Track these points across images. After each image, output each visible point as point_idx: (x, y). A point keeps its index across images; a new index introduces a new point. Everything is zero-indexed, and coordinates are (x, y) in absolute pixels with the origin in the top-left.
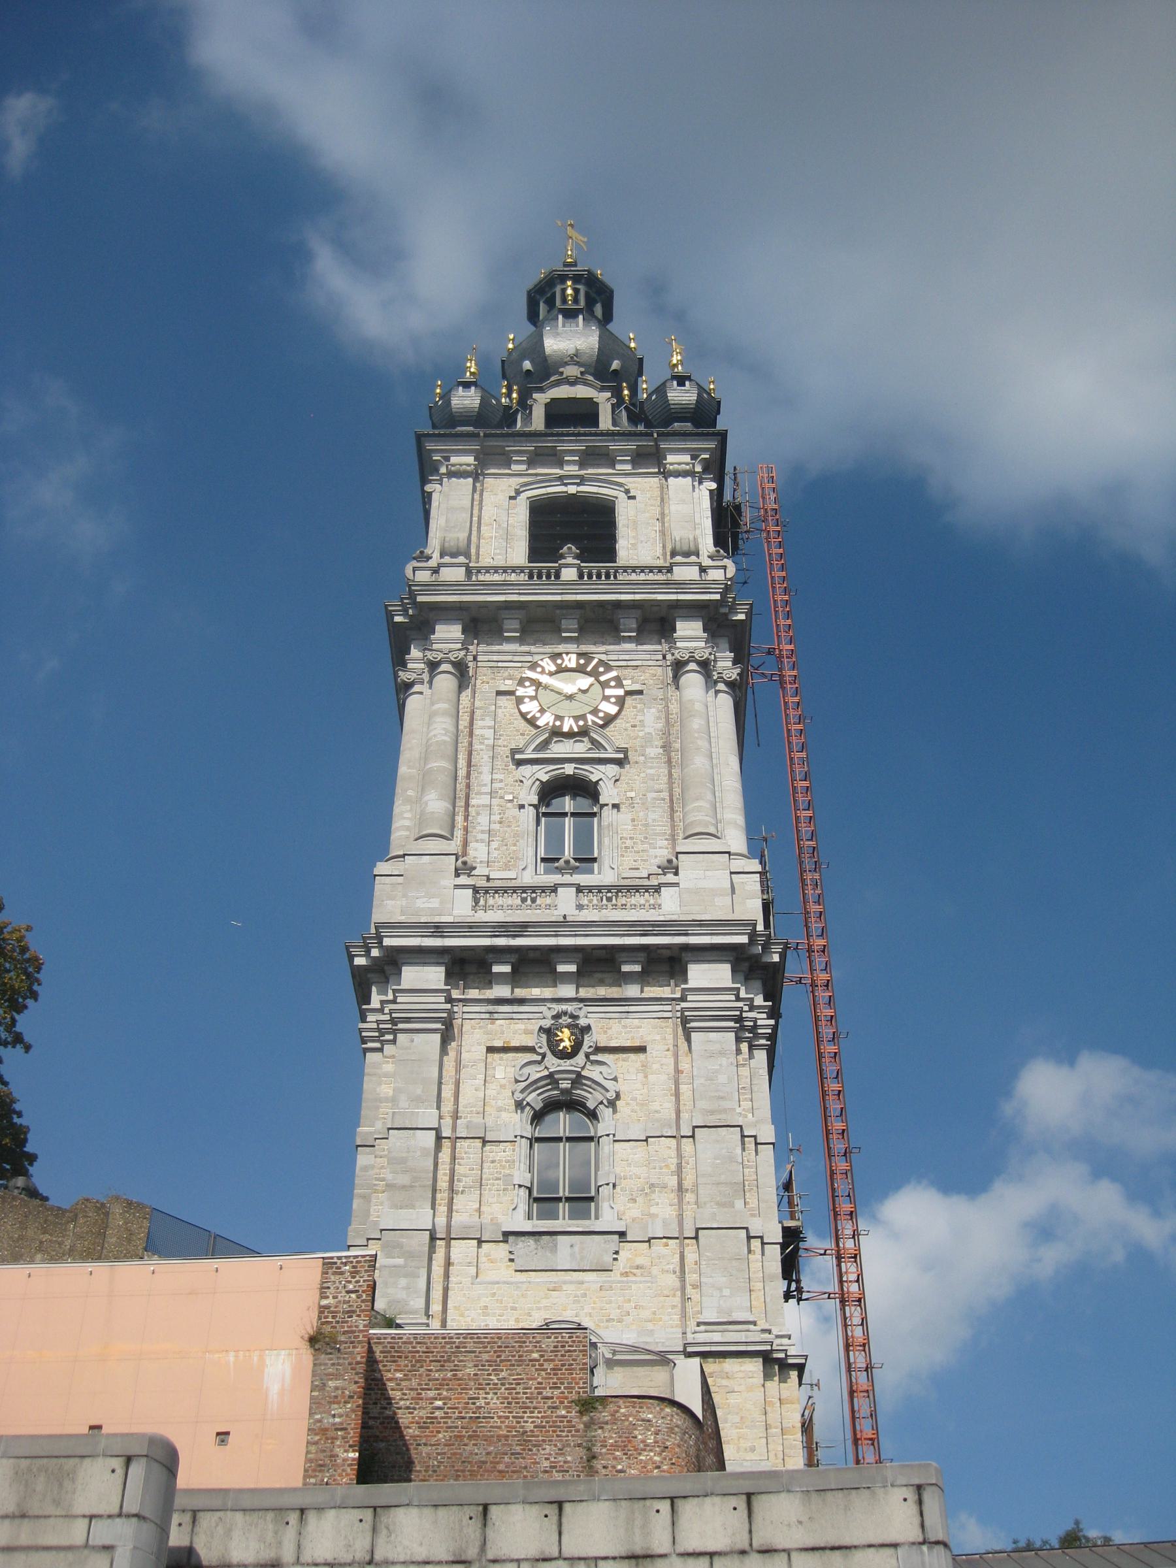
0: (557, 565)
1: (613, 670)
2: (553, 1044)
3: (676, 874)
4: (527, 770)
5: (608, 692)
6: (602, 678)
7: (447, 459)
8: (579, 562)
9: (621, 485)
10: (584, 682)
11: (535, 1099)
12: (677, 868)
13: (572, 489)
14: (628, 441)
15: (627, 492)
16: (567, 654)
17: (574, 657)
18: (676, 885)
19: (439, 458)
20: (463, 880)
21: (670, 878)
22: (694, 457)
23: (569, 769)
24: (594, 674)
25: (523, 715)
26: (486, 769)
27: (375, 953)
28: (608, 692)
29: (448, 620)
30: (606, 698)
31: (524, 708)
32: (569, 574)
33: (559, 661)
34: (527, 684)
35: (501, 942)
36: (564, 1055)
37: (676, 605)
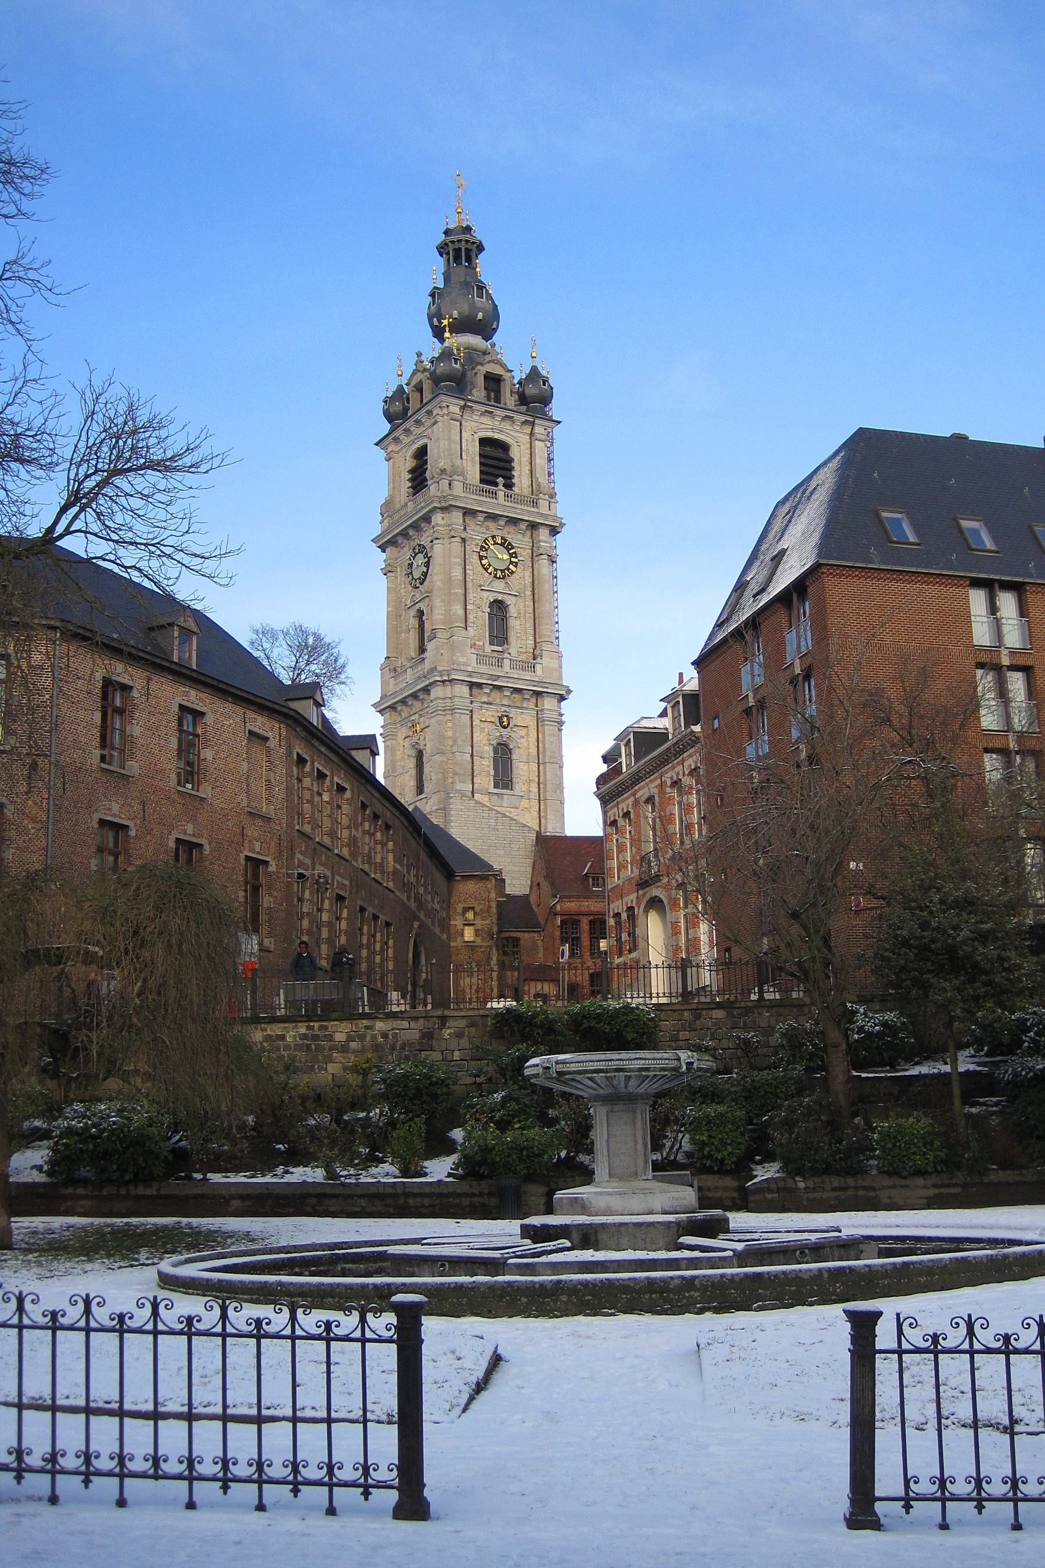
2: (501, 723)
4: (485, 594)
5: (513, 559)
6: (511, 552)
7: (448, 406)
10: (506, 557)
11: (494, 742)
13: (496, 436)
20: (473, 650)
24: (508, 550)
25: (483, 566)
26: (471, 592)
27: (446, 678)
28: (513, 559)
30: (511, 563)
31: (484, 562)
32: (501, 494)
35: (490, 682)
36: (505, 727)
37: (542, 524)
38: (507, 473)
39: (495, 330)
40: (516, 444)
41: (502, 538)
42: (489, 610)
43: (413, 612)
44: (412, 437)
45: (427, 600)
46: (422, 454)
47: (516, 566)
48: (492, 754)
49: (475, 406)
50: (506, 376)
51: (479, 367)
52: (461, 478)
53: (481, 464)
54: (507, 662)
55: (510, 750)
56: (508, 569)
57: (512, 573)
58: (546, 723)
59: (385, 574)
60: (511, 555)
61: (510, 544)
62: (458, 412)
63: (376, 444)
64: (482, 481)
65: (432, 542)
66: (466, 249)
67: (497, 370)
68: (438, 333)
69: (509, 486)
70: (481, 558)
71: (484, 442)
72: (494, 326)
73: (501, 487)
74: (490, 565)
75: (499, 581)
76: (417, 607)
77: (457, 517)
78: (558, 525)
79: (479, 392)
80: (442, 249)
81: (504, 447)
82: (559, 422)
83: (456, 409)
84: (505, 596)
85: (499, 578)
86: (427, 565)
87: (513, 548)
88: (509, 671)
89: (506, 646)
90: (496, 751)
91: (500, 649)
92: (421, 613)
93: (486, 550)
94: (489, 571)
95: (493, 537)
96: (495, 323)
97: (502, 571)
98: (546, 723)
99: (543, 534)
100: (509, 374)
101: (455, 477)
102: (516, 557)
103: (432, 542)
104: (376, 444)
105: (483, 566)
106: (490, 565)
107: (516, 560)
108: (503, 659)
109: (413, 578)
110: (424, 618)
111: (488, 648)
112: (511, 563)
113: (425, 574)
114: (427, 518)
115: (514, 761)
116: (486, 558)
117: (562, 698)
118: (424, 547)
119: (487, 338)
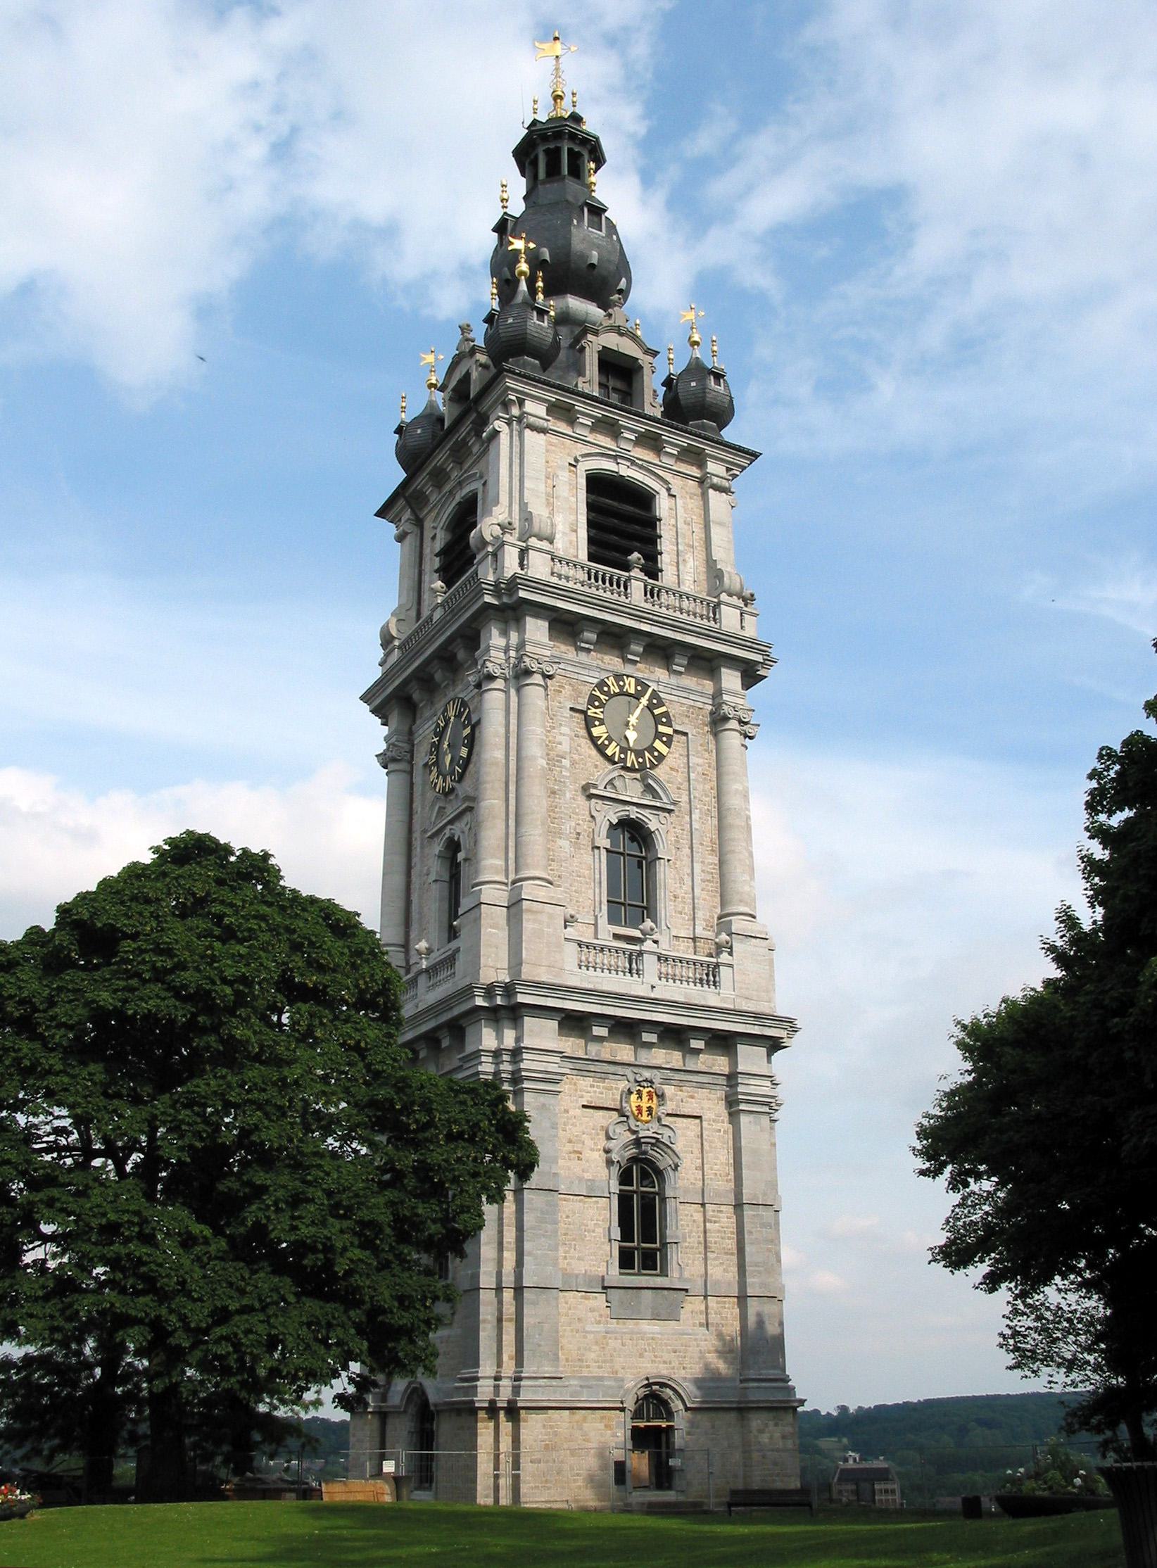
0: (627, 574)
1: (664, 705)
3: (731, 954)
5: (661, 729)
6: (656, 712)
7: (521, 403)
8: (646, 578)
9: (666, 482)
12: (731, 948)
13: (625, 471)
14: (678, 435)
15: (669, 490)
16: (628, 676)
17: (633, 680)
18: (731, 966)
19: (514, 398)
20: (571, 932)
21: (724, 957)
22: (728, 470)
23: (634, 813)
27: (499, 1001)
28: (661, 729)
29: (536, 616)
30: (658, 735)
31: (596, 731)
32: (637, 588)
33: (621, 683)
34: (597, 703)
38: (649, 548)
39: (624, 293)
40: (664, 493)
41: (638, 682)
42: (607, 843)
43: (438, 847)
44: (447, 488)
45: (467, 817)
46: (467, 514)
47: (668, 744)
48: (615, 1187)
49: (579, 407)
50: (644, 359)
51: (590, 337)
52: (544, 545)
53: (591, 524)
54: (650, 963)
55: (660, 1173)
56: (651, 749)
57: (661, 758)
58: (742, 1107)
59: (385, 767)
60: (657, 720)
61: (655, 694)
62: (544, 414)
63: (380, 514)
64: (592, 557)
65: (479, 686)
66: (569, 150)
67: (627, 347)
68: (506, 287)
69: (652, 571)
70: (589, 723)
71: (599, 485)
72: (623, 284)
73: (636, 573)
74: (610, 739)
75: (628, 775)
76: (447, 832)
77: (537, 629)
78: (759, 658)
79: (590, 380)
80: (524, 155)
81: (644, 499)
82: (755, 455)
83: (541, 410)
84: (646, 812)
85: (631, 770)
86: (471, 742)
87: (661, 704)
88: (655, 981)
89: (648, 923)
90: (625, 1178)
91: (637, 933)
92: (453, 846)
93: (602, 705)
94: (609, 752)
95: (619, 677)
96: (624, 280)
97: (639, 754)
98: (742, 1107)
99: (731, 679)
100: (650, 359)
101: (533, 541)
102: (669, 724)
103: (479, 686)
104: (380, 514)
105: (593, 740)
106: (610, 739)
107: (669, 731)
108: (641, 953)
109: (439, 773)
110: (461, 856)
111: (607, 931)
112: (658, 735)
113: (468, 761)
114: (471, 638)
115: (670, 1205)
116: (602, 722)
117: (774, 1045)
118: (464, 704)
119: (605, 305)
